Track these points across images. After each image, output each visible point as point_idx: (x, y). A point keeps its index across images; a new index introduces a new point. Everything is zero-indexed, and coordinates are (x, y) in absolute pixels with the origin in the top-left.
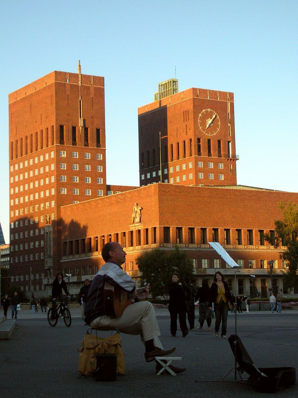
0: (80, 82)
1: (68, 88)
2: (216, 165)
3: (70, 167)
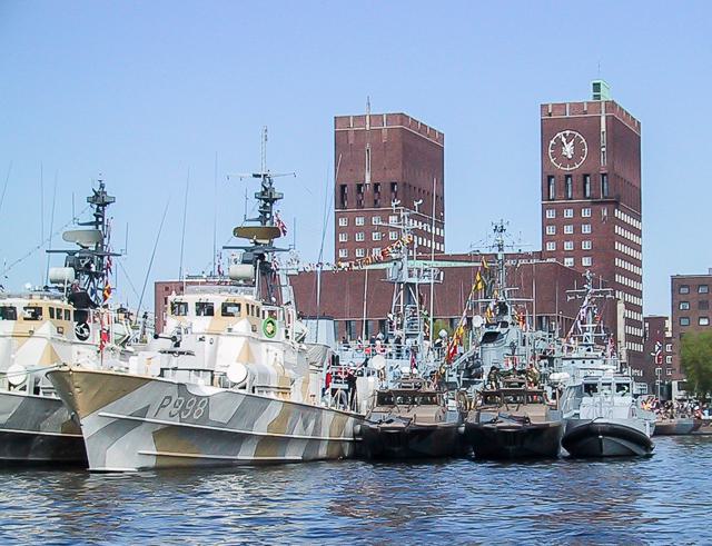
0: (368, 126)
1: (351, 135)
2: (577, 212)
3: (351, 239)
